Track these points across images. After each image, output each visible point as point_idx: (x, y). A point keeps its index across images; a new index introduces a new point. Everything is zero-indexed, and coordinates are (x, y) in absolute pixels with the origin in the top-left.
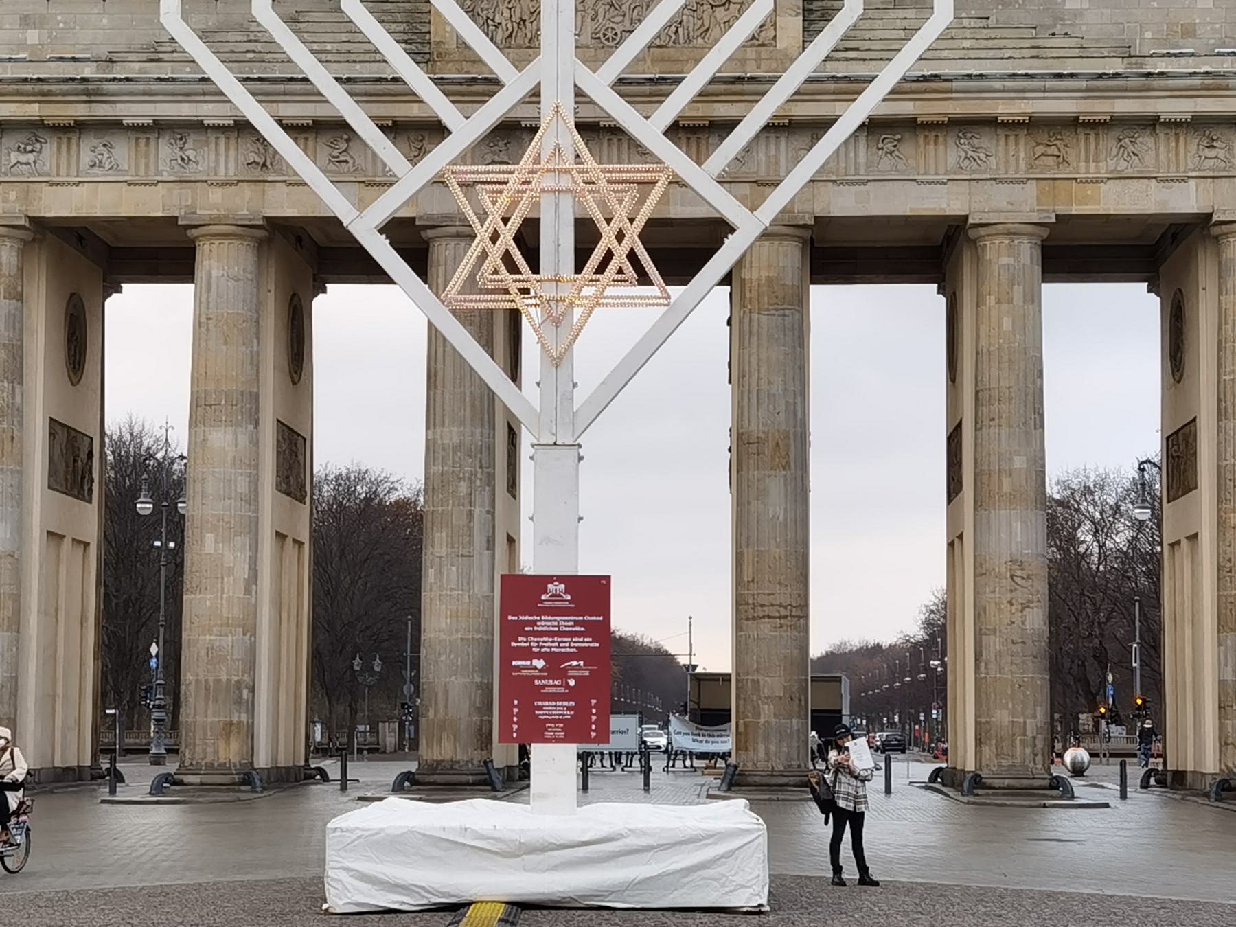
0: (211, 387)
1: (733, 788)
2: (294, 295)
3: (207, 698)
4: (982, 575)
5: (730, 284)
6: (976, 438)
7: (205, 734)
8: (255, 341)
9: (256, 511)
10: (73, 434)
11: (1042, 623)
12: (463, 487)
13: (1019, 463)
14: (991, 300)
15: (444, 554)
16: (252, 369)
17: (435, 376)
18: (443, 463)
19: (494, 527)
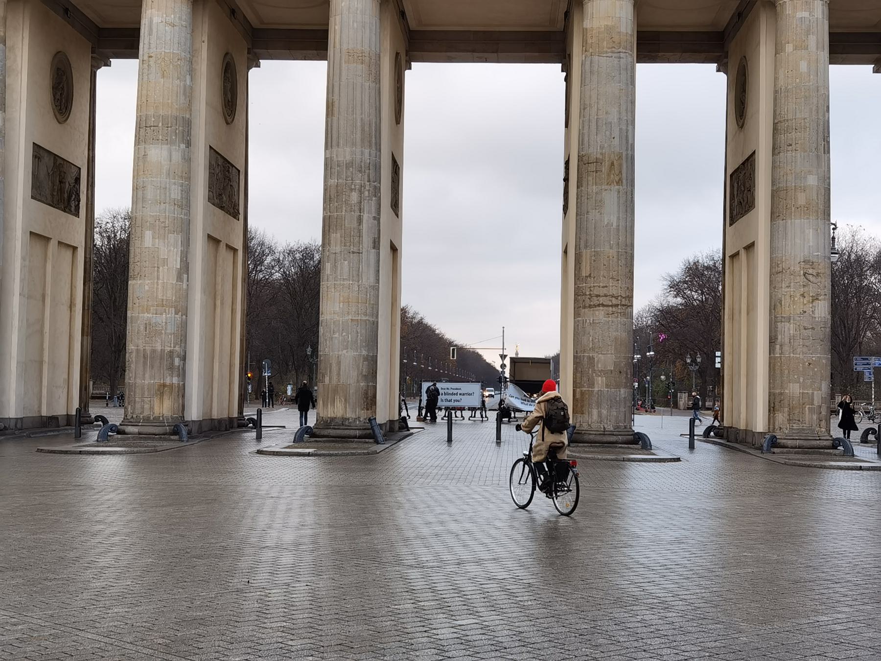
0: (151, 112)
1: (572, 445)
2: (227, 54)
3: (145, 364)
4: (777, 273)
5: (563, 57)
6: (774, 162)
7: (143, 394)
8: (188, 77)
9: (188, 213)
10: (59, 161)
11: (827, 313)
12: (354, 197)
13: (812, 180)
14: (789, 48)
15: (338, 251)
16: (185, 99)
17: (333, 105)
18: (339, 176)
19: (379, 231)
